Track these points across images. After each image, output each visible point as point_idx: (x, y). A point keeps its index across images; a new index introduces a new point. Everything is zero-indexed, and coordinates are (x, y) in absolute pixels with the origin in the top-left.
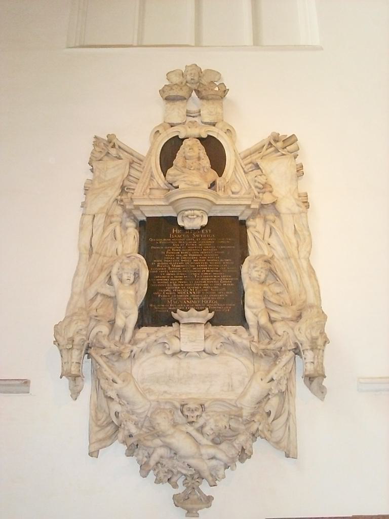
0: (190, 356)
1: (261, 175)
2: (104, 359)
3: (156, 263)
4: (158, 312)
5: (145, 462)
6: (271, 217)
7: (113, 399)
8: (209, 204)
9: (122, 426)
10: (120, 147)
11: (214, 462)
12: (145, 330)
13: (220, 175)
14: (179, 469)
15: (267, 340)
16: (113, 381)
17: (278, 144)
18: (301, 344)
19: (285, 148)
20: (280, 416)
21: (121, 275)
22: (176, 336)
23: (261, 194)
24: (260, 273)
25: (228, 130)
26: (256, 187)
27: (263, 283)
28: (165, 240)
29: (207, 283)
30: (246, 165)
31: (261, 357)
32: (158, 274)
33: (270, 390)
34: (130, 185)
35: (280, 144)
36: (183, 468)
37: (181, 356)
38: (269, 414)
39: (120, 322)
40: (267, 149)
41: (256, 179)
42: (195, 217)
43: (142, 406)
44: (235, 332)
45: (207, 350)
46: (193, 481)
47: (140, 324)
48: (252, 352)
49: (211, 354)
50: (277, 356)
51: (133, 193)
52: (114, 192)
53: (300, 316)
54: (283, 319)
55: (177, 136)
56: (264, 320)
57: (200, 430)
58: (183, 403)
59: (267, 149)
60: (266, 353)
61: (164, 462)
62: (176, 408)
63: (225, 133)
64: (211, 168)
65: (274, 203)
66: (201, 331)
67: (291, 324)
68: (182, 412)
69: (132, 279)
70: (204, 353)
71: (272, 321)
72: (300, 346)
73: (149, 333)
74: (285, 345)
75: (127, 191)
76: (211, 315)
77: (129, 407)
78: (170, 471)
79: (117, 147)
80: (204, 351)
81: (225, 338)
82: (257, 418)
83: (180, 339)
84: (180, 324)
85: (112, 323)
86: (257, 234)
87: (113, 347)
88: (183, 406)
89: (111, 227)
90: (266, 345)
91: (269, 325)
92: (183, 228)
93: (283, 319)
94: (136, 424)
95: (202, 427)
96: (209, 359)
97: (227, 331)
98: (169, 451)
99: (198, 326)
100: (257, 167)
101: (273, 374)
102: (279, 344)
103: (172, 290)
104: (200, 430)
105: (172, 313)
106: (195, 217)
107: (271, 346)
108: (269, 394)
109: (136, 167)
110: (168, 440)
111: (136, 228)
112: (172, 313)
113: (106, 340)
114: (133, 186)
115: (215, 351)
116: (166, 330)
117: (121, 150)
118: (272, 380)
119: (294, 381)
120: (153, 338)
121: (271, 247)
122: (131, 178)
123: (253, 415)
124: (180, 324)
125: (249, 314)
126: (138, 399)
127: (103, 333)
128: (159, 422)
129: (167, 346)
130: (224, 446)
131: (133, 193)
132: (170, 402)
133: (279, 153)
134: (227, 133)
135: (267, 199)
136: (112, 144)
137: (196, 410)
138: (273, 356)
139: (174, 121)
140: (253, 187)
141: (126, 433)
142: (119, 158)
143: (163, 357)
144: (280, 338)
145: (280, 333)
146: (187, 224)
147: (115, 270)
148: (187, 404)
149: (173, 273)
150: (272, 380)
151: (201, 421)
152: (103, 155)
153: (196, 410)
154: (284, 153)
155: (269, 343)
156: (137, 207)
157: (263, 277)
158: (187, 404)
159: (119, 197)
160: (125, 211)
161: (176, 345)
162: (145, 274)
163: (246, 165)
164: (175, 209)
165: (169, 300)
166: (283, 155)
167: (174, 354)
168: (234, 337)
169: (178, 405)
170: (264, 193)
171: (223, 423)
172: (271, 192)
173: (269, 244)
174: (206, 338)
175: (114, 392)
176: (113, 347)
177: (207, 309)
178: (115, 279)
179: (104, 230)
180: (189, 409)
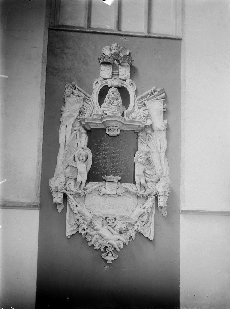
0: (110, 196)
1: (146, 110)
2: (72, 196)
3: (96, 152)
4: (96, 175)
5: (90, 241)
6: (149, 131)
7: (76, 214)
8: (121, 124)
9: (81, 225)
10: (78, 90)
11: (119, 241)
12: (91, 184)
13: (127, 109)
14: (104, 244)
15: (144, 191)
16: (76, 206)
17: (155, 93)
18: (158, 193)
19: (159, 96)
20: (147, 223)
21: (79, 157)
22: (104, 187)
23: (145, 120)
24: (142, 160)
25: (132, 84)
26: (144, 116)
27: (143, 165)
28: (100, 141)
29: (118, 163)
30: (139, 104)
31: (141, 198)
32: (97, 157)
33: (144, 212)
34: (83, 111)
35: (156, 93)
36: (106, 244)
37: (106, 196)
38: (143, 222)
39: (79, 179)
40: (150, 96)
41: (144, 111)
42: (114, 130)
43: (89, 216)
44: (130, 187)
45: (117, 194)
46: (110, 249)
47: (88, 181)
48: (138, 196)
49: (120, 196)
50: (148, 198)
51: (85, 115)
52: (76, 114)
53: (159, 180)
54: (152, 181)
55: (107, 85)
56: (143, 182)
57: (114, 228)
58: (107, 217)
59: (150, 96)
60: (143, 196)
61: (99, 241)
62: (104, 219)
63: (131, 85)
64: (123, 104)
65: (151, 125)
66: (115, 185)
67: (155, 183)
68: (106, 220)
69: (85, 160)
70: (116, 195)
71: (147, 182)
72: (158, 193)
73: (92, 185)
74: (152, 193)
75: (82, 114)
76: (120, 178)
77: (84, 217)
78: (100, 244)
79: (77, 89)
80: (116, 194)
81: (125, 189)
82: (138, 224)
83: (106, 188)
84: (106, 181)
85: (76, 179)
86: (142, 140)
87: (76, 190)
88: (106, 218)
89: (75, 132)
90: (143, 192)
91: (145, 184)
92: (108, 135)
93: (152, 181)
94: (86, 225)
95: (114, 227)
96: (119, 198)
97: (126, 186)
98: (100, 237)
99: (114, 183)
100: (145, 105)
101: (145, 205)
102: (149, 192)
103: (103, 165)
104: (114, 228)
105: (103, 176)
106: (114, 130)
107: (145, 193)
108: (143, 214)
109: (87, 101)
110: (100, 232)
111: (87, 134)
112: (103, 176)
113: (73, 187)
114: (85, 112)
115: (121, 195)
116: (100, 184)
117: (79, 92)
118: (145, 208)
119: (150, 159)
120: (94, 187)
121: (148, 147)
122: (84, 107)
123: (136, 222)
124: (106, 181)
125: (136, 178)
126: (88, 214)
127: (72, 184)
128: (96, 225)
129: (100, 191)
130: (123, 235)
131: (85, 115)
132: (101, 216)
133: (156, 98)
134: (131, 85)
135: (149, 123)
136: (74, 88)
137: (112, 220)
138: (146, 198)
139: (106, 77)
140: (142, 116)
141: (82, 228)
142: (78, 96)
143: (99, 196)
144: (150, 189)
145: (150, 187)
146: (111, 133)
147: (76, 155)
148: (108, 217)
149: (103, 157)
150: (145, 208)
151: (114, 225)
152: (70, 93)
153: (112, 220)
154: (158, 98)
155: (145, 192)
156: (87, 123)
157: (144, 161)
158: (108, 217)
159: (78, 117)
160: (81, 125)
161: (103, 191)
162: (90, 157)
163: (139, 104)
164: (105, 126)
165: (102, 170)
166: (158, 99)
167: (103, 195)
168: (130, 189)
169: (105, 218)
170: (147, 119)
171: (123, 226)
172: (150, 119)
173: (148, 145)
174: (117, 188)
175: (77, 211)
176: (76, 190)
177: (118, 176)
178: (77, 159)
179: (71, 133)
180: (109, 220)
